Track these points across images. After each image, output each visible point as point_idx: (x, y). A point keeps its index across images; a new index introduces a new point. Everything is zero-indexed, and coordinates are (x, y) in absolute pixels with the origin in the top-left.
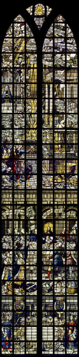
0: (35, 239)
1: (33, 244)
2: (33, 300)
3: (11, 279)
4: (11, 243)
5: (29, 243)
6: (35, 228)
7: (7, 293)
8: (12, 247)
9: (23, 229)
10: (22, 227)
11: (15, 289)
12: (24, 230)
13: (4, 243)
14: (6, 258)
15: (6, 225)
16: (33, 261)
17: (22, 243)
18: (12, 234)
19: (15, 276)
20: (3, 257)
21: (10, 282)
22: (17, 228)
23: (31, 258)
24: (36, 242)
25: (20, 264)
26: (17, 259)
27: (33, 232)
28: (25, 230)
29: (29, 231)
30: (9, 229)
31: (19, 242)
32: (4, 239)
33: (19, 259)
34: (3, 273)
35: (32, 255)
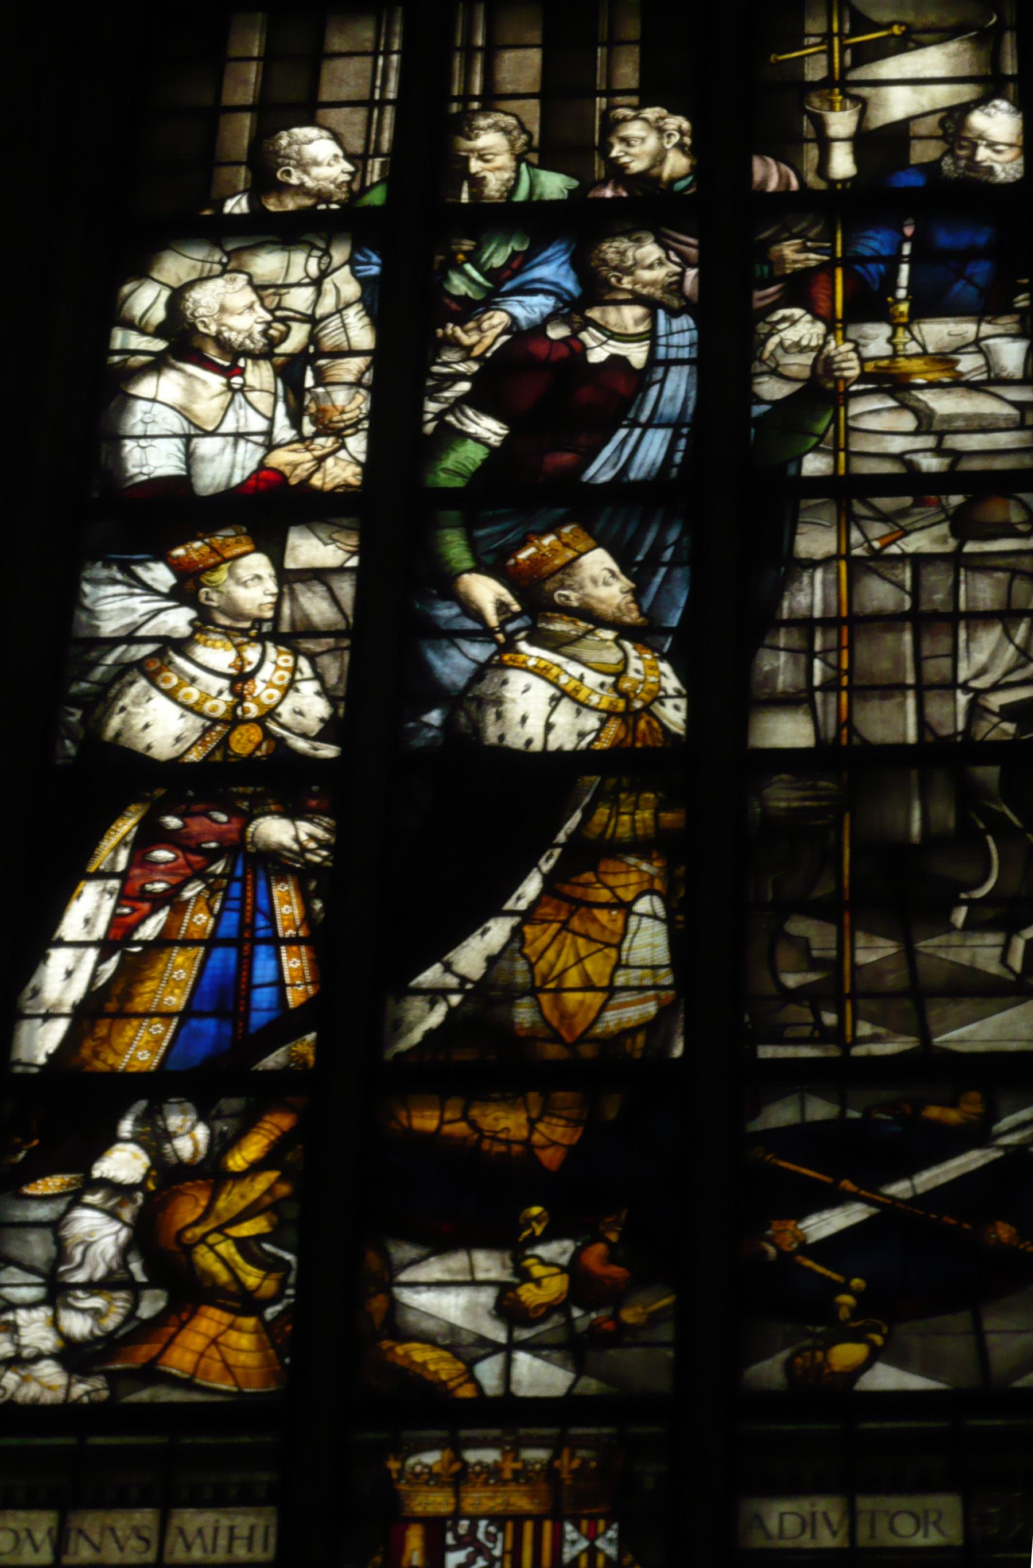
0: (981, 270)
1: (945, 359)
2: (949, 1504)
3: (274, 1060)
4: (351, 367)
5: (839, 349)
6: (966, 92)
7: (145, 1352)
8: (357, 444)
9: (651, 113)
10: (628, 74)
11: (403, 1252)
12: (676, 122)
13: (158, 364)
14: (181, 646)
15: (252, 72)
16: (937, 669)
17: (637, 354)
18: (377, 197)
19: (431, 976)
20: (108, 627)
21: (232, 1104)
22: (531, 110)
23: (890, 621)
24: (1008, 323)
25: (564, 739)
26: (480, 652)
27: (923, 152)
28: (694, 134)
29: (825, 143)
30: (311, 121)
31: (557, 332)
32: (177, 296)
33: (556, 643)
34: (71, 927)
35: (918, 561)
